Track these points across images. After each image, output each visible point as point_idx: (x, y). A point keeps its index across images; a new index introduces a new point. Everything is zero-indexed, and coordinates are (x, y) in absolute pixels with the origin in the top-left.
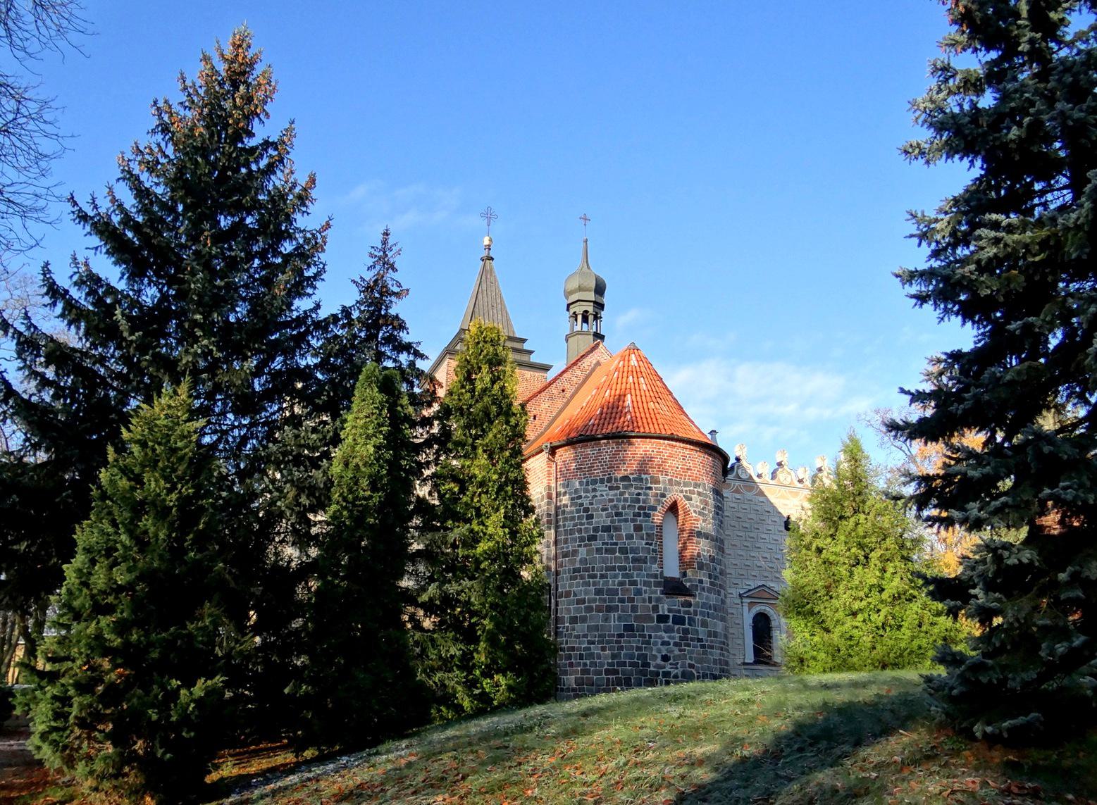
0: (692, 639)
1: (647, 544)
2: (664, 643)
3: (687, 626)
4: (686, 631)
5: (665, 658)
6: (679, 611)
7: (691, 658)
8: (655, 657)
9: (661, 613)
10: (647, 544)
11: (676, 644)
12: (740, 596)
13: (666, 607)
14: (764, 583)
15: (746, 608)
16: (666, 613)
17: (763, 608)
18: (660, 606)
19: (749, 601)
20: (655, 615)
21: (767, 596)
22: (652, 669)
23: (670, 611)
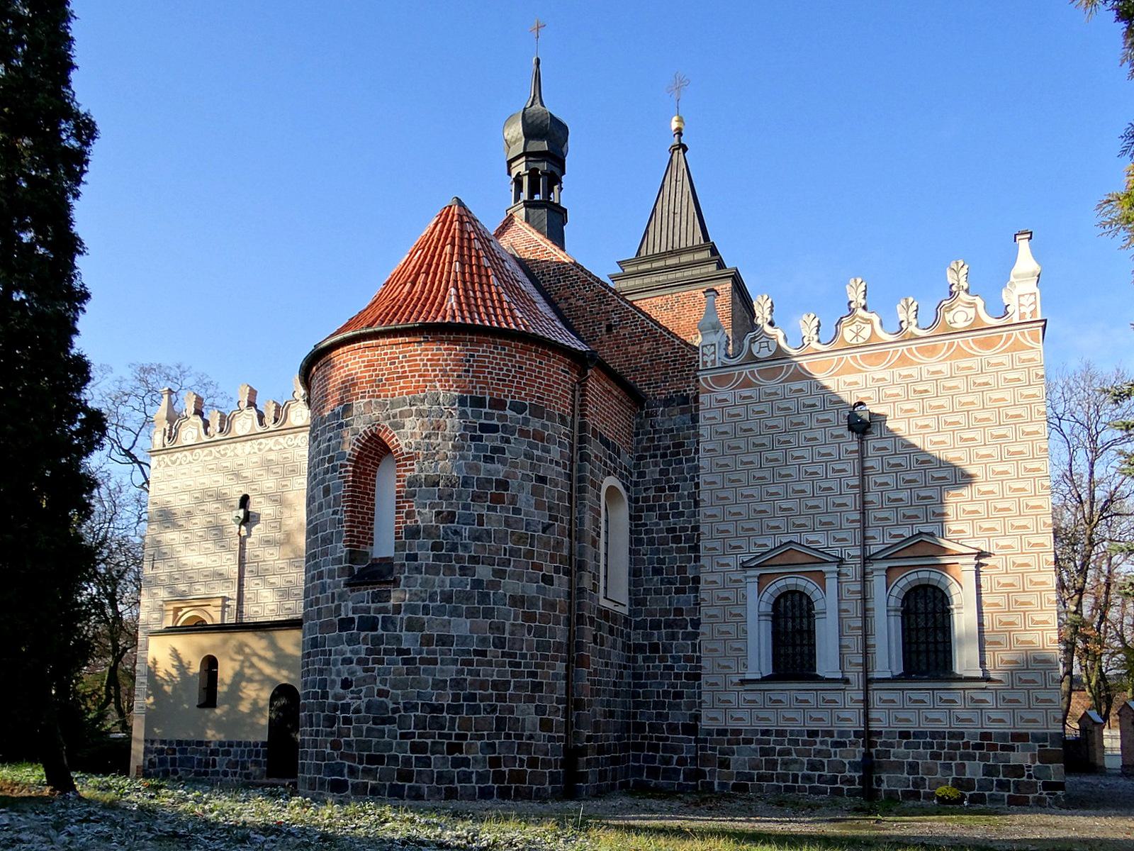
0: (386, 652)
1: (335, 513)
2: (347, 661)
3: (380, 632)
4: (378, 640)
5: (346, 684)
6: (367, 610)
7: (384, 682)
8: (333, 682)
9: (343, 616)
10: (335, 513)
11: (360, 662)
12: (744, 566)
13: (350, 604)
14: (795, 538)
15: (752, 587)
16: (351, 615)
17: (790, 581)
18: (343, 604)
19: (758, 572)
20: (336, 620)
21: (800, 559)
22: (330, 700)
23: (355, 611)
